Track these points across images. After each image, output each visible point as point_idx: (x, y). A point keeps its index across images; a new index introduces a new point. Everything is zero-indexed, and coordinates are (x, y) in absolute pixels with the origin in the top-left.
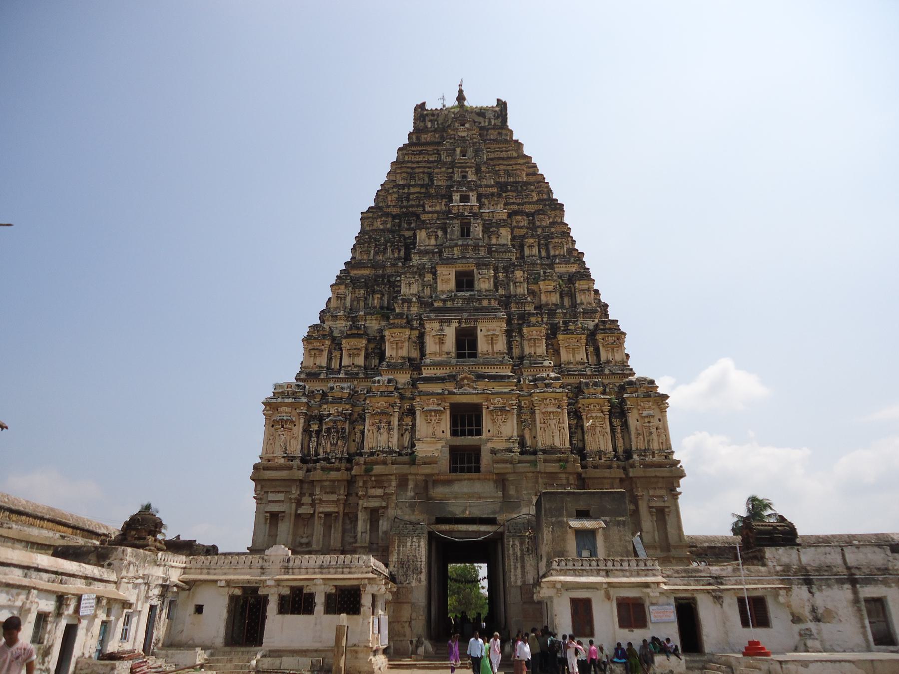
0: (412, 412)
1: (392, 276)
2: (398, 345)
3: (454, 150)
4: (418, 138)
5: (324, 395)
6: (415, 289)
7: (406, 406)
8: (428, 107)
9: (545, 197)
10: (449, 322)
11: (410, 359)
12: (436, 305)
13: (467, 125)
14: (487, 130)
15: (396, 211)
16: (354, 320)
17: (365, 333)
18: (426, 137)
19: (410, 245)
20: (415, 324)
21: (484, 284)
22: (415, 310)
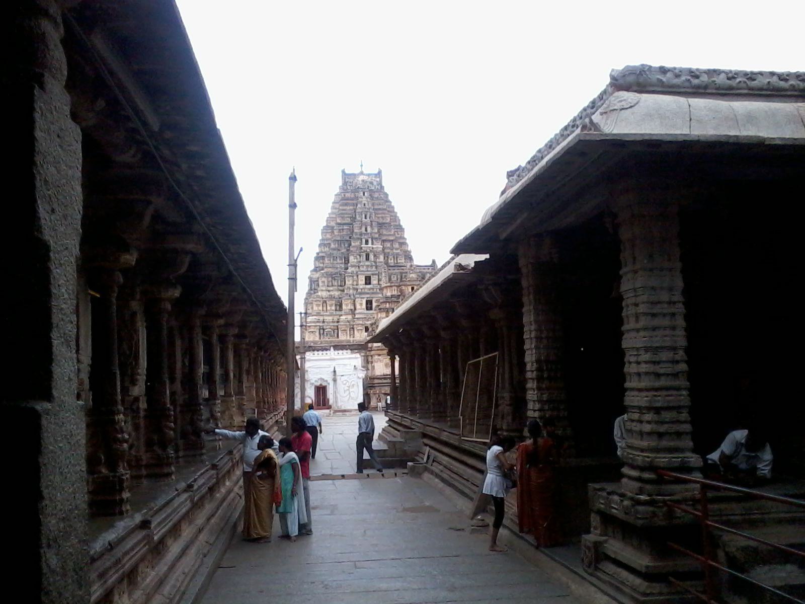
0: (353, 328)
1: (340, 271)
2: (347, 305)
3: (362, 215)
4: (344, 195)
5: (324, 322)
6: (351, 283)
7: (352, 326)
8: (347, 172)
9: (398, 223)
10: (364, 298)
11: (351, 310)
12: (359, 290)
13: (366, 194)
14: (374, 192)
15: (339, 238)
16: (329, 291)
17: (334, 297)
18: (348, 195)
19: (347, 261)
20: (352, 297)
21: (374, 281)
22: (351, 291)
